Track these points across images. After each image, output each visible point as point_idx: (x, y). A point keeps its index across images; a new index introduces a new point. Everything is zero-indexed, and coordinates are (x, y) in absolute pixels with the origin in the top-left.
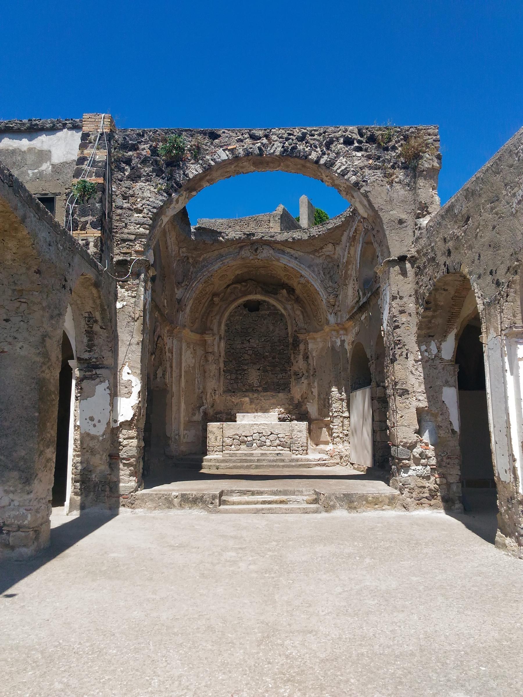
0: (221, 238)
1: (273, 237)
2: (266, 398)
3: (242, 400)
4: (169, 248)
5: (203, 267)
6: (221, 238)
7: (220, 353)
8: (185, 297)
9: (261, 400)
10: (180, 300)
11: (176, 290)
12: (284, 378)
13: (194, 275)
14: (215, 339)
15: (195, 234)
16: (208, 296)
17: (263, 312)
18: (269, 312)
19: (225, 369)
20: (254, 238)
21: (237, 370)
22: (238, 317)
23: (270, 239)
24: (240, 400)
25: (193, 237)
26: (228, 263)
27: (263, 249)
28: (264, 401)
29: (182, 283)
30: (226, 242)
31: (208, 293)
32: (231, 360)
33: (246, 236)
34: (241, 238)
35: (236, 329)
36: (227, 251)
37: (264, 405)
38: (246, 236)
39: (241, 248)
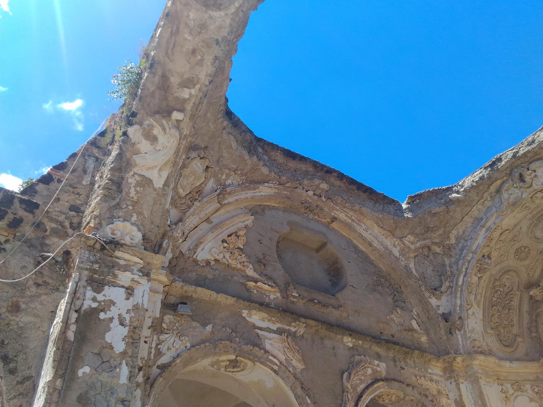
0: (454, 195)
1: (533, 141)
4: (375, 244)
5: (462, 250)
6: (454, 195)
8: (455, 305)
10: (450, 313)
11: (434, 301)
13: (455, 267)
15: (410, 210)
16: (519, 293)
20: (503, 163)
23: (530, 148)
25: (409, 215)
26: (495, 224)
27: (535, 171)
29: (441, 287)
30: (466, 196)
31: (515, 289)
33: (489, 169)
34: (483, 176)
36: (484, 209)
38: (489, 169)
39: (498, 191)
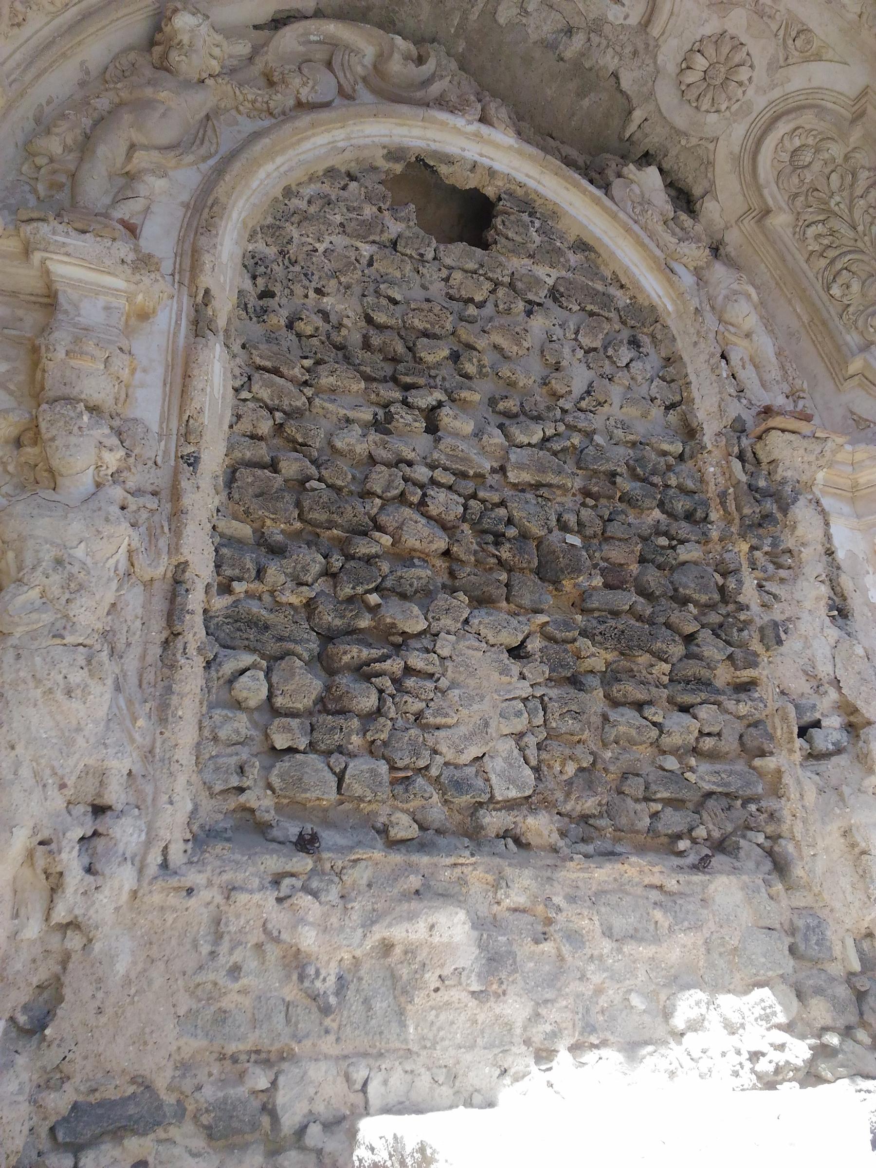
2: (619, 923)
3: (399, 933)
7: (187, 434)
9: (575, 937)
12: (708, 743)
14: (144, 316)
17: (518, 264)
18: (555, 274)
19: (220, 603)
21: (328, 637)
22: (340, 241)
24: (379, 933)
28: (606, 946)
32: (276, 531)
35: (325, 315)
37: (612, 994)
